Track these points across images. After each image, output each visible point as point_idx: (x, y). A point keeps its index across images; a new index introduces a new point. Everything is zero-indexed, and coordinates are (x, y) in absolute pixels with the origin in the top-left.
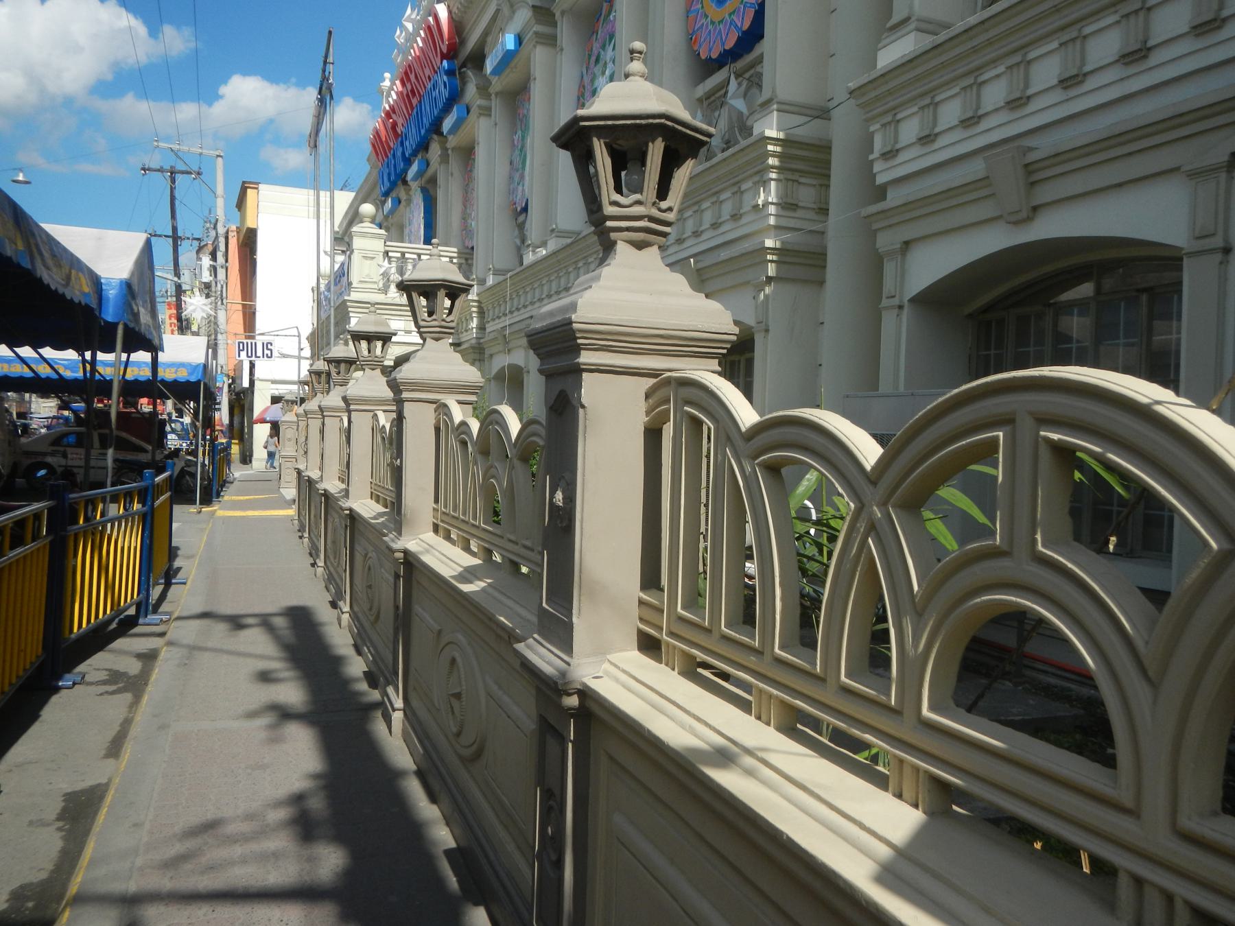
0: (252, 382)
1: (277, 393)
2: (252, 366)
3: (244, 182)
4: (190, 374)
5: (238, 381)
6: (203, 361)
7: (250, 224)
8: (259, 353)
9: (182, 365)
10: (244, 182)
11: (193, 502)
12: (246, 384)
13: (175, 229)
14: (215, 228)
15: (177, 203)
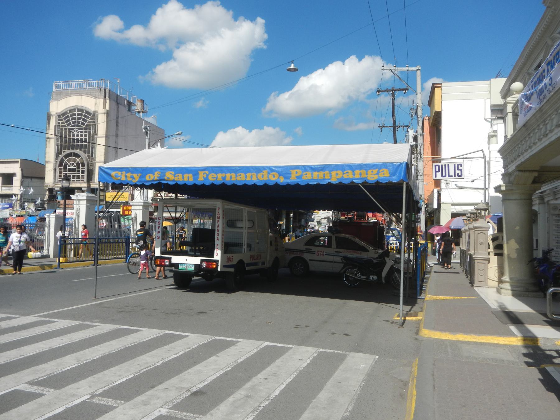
0: (439, 205)
1: (455, 211)
2: (439, 195)
3: (433, 84)
4: (392, 174)
5: (430, 206)
6: (406, 161)
7: (437, 109)
8: (452, 173)
9: (384, 165)
10: (433, 84)
11: (398, 303)
12: (435, 206)
13: (394, 122)
14: (416, 113)
15: (396, 107)
